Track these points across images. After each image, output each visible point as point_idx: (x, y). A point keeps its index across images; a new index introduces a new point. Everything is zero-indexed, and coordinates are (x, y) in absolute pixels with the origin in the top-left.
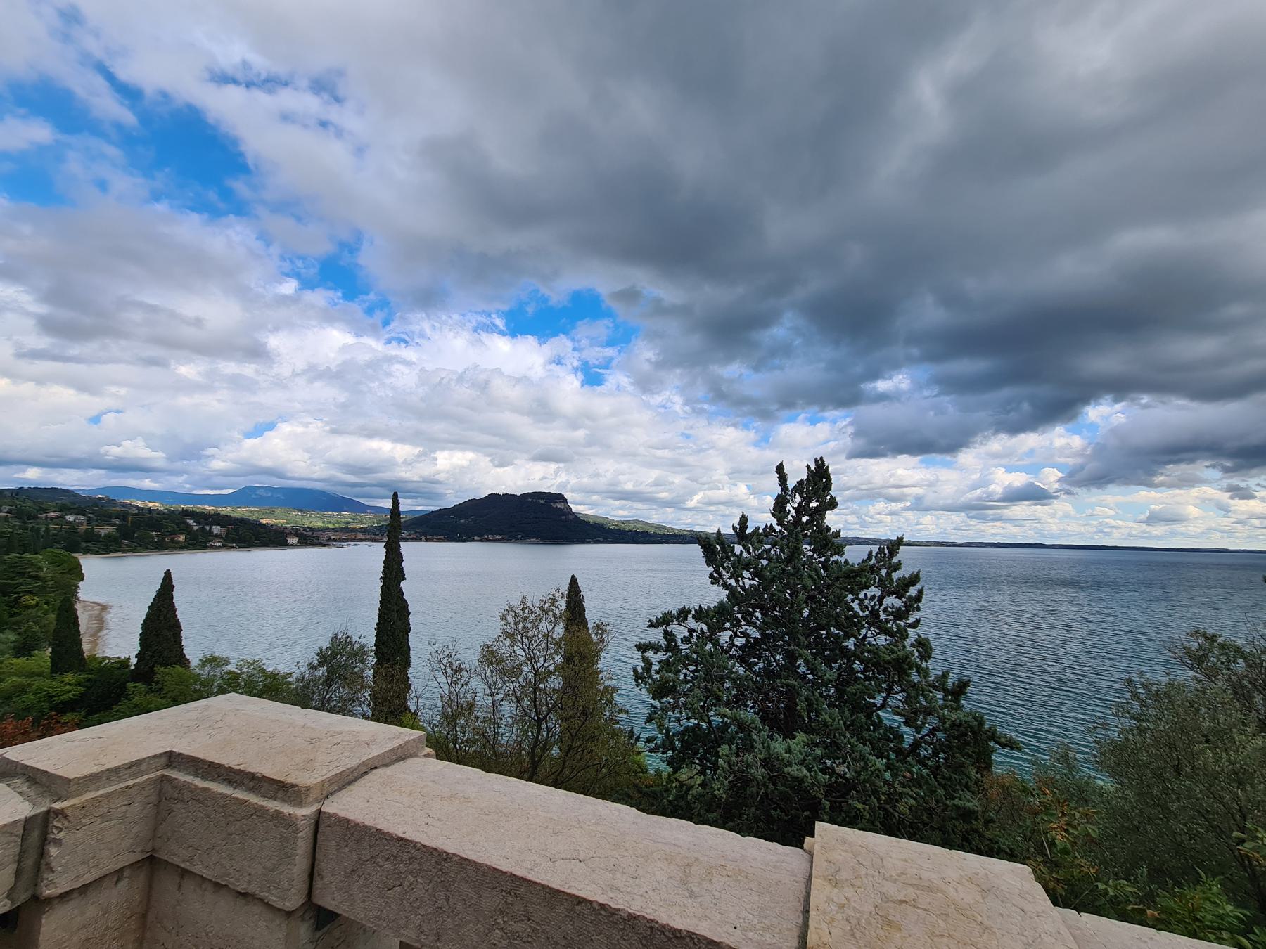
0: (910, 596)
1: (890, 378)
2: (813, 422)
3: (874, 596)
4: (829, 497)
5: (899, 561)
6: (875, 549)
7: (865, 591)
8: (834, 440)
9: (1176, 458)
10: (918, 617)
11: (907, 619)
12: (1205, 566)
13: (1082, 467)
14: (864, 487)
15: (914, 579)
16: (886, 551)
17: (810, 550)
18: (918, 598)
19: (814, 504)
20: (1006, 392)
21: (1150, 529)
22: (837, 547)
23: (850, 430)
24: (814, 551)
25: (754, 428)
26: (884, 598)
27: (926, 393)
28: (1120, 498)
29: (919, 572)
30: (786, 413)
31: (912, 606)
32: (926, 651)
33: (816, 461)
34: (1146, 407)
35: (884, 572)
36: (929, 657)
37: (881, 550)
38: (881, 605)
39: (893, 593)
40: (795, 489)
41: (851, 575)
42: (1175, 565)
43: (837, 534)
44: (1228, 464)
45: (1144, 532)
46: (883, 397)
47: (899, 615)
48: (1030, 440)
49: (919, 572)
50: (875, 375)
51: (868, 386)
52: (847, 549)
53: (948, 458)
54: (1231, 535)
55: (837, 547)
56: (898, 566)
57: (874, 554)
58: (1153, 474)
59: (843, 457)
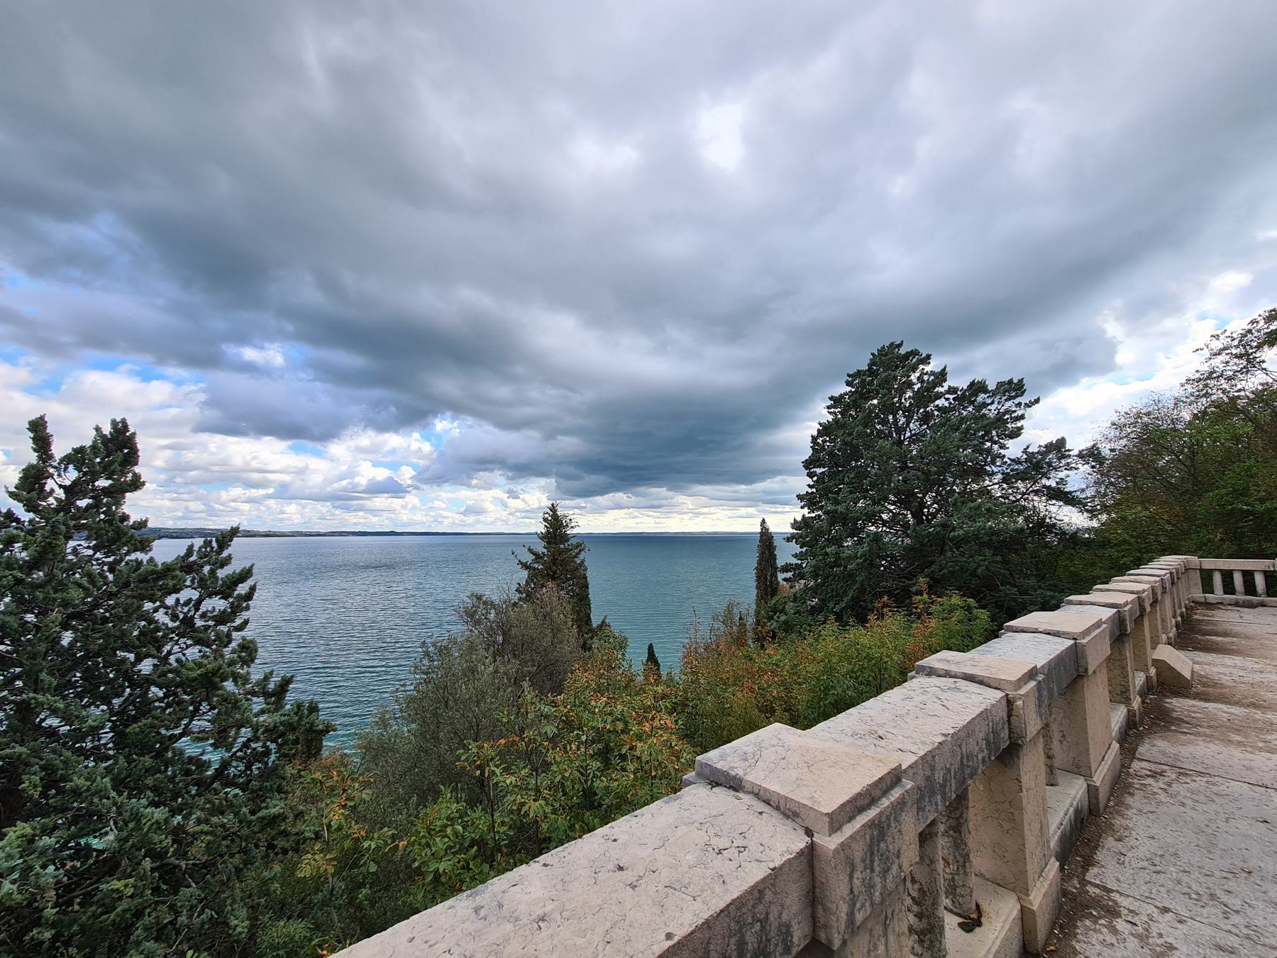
0: (239, 595)
1: (262, 348)
2: (147, 377)
3: (190, 600)
4: (130, 475)
5: (230, 555)
6: (198, 542)
7: (174, 596)
8: (179, 407)
9: (483, 467)
10: (246, 618)
11: (233, 621)
12: (488, 545)
13: (428, 468)
14: (216, 468)
15: (245, 575)
16: (214, 544)
17: (88, 547)
18: (249, 596)
19: (103, 483)
20: (376, 393)
21: (465, 518)
22: (140, 542)
23: (202, 397)
24: (96, 549)
25: (28, 364)
26: (203, 600)
27: (302, 375)
28: (450, 495)
29: (252, 566)
30: (92, 354)
31: (239, 606)
32: (250, 655)
33: (114, 423)
34: (471, 427)
35: (207, 569)
36: (253, 661)
37: (207, 544)
38: (197, 609)
39: (216, 594)
40: (68, 460)
41: (150, 577)
42: (473, 545)
43: (142, 524)
44: (510, 474)
45: (462, 521)
46: (248, 368)
47: (222, 618)
48: (393, 440)
49: (252, 566)
50: (242, 338)
51: (230, 350)
52: (156, 544)
53: (318, 446)
54: (506, 522)
55: (140, 542)
56: (226, 562)
57: (196, 548)
58: (471, 477)
59: (187, 430)
